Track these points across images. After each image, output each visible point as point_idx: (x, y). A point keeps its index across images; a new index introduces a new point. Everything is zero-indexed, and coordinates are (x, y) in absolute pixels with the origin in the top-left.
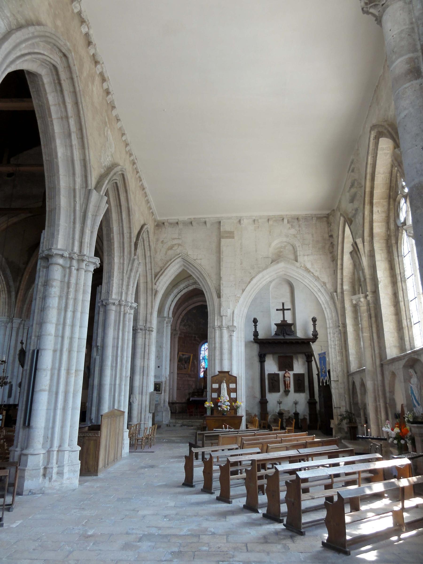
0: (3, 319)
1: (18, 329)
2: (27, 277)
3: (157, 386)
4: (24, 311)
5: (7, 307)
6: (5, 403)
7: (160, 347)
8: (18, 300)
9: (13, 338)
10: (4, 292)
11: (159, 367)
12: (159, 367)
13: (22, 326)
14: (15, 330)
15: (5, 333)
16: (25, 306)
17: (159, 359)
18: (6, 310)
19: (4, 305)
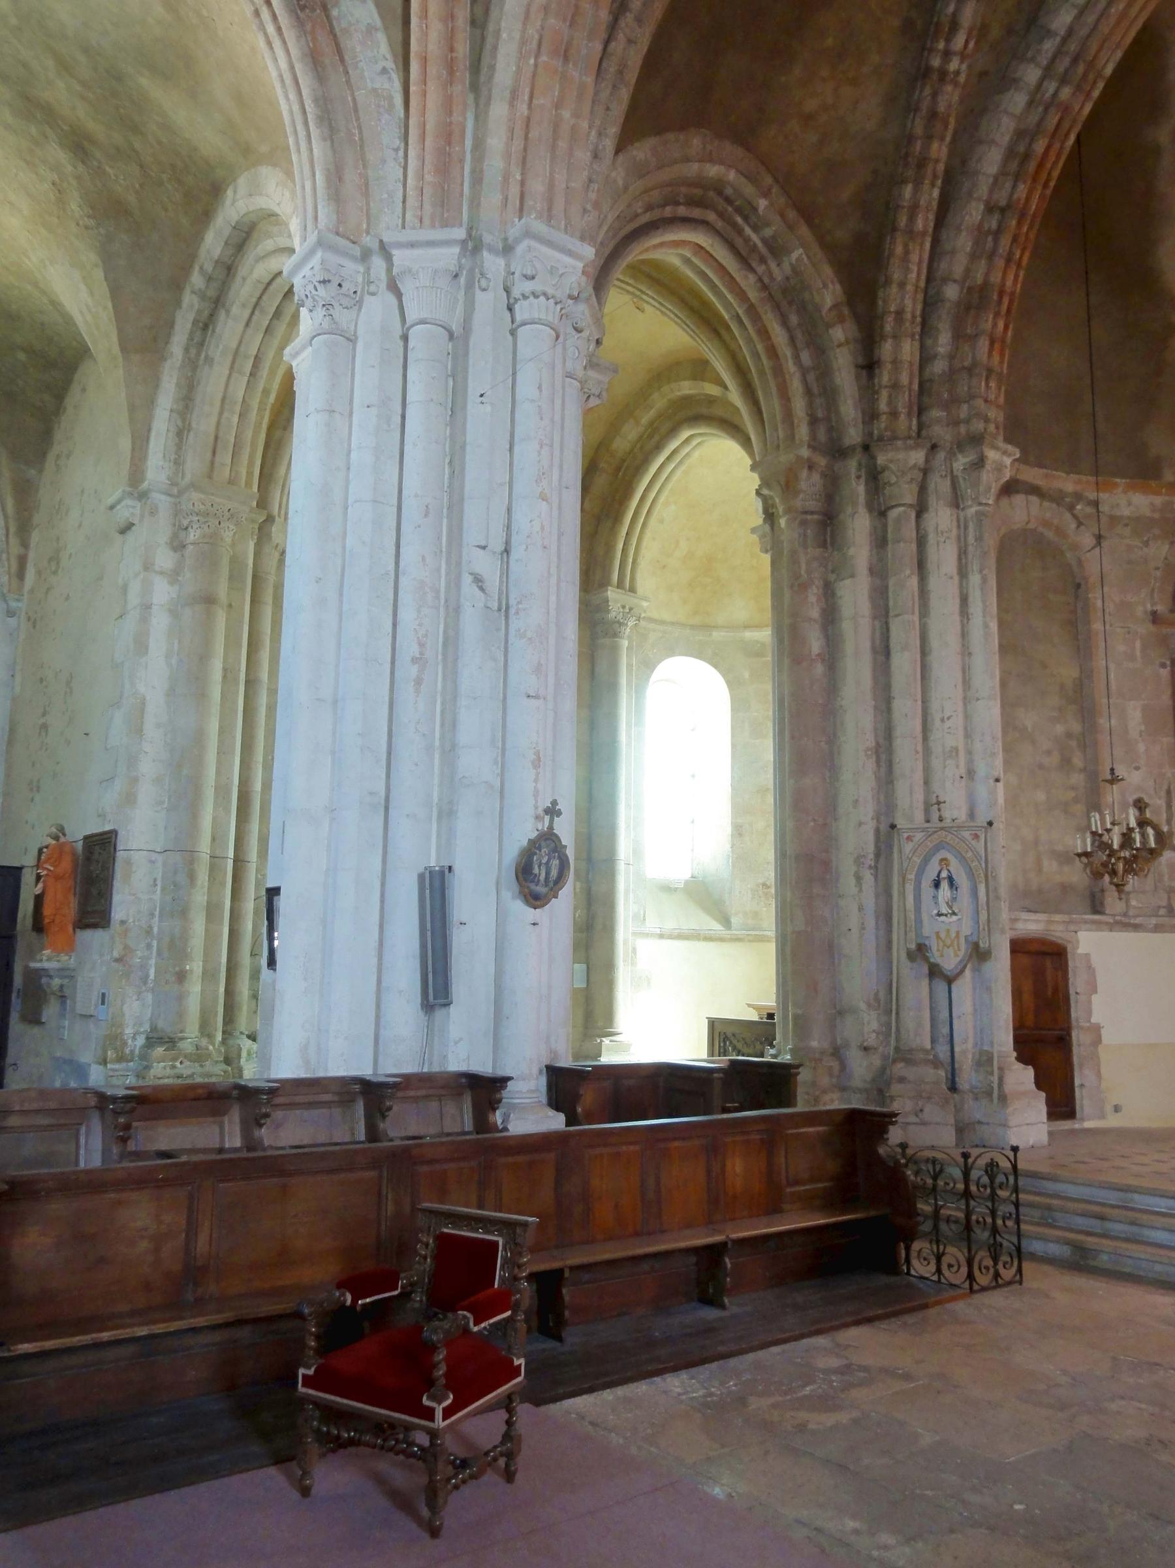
6: (400, 1059)
13: (488, 302)
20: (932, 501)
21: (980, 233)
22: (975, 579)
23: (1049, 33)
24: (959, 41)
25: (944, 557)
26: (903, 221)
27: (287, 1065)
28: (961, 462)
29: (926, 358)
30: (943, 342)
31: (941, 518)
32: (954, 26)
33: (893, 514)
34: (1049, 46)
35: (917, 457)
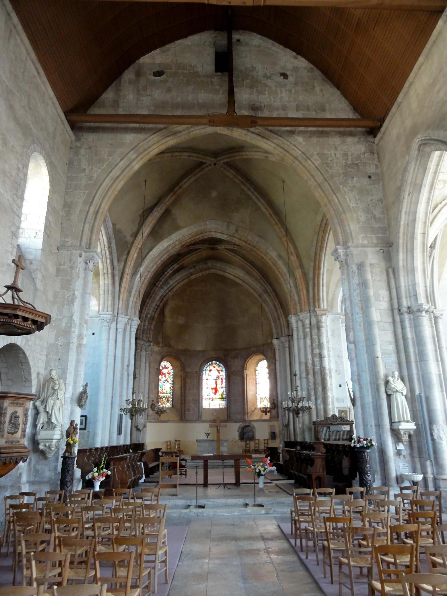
0: (105, 316)
1: (125, 330)
2: (135, 255)
3: (343, 414)
4: (130, 306)
5: (110, 298)
6: (114, 444)
7: (339, 356)
8: (122, 289)
9: (119, 344)
10: (106, 275)
11: (340, 386)
12: (340, 386)
13: (129, 327)
14: (120, 332)
15: (109, 338)
16: (132, 298)
17: (339, 374)
18: (110, 302)
19: (106, 296)
20: (143, 350)
21: (154, 308)
22: (147, 364)
23: (168, 283)
24: (161, 283)
25: (143, 360)
26: (146, 304)
27: (98, 445)
28: (147, 344)
29: (144, 326)
30: (147, 323)
31: (144, 353)
32: (161, 281)
33: (138, 351)
34: (169, 285)
35: (142, 342)
